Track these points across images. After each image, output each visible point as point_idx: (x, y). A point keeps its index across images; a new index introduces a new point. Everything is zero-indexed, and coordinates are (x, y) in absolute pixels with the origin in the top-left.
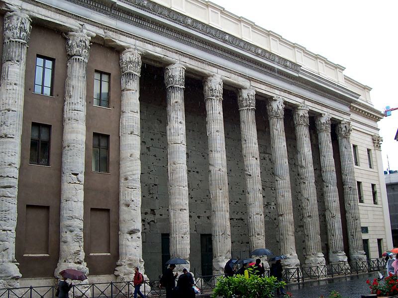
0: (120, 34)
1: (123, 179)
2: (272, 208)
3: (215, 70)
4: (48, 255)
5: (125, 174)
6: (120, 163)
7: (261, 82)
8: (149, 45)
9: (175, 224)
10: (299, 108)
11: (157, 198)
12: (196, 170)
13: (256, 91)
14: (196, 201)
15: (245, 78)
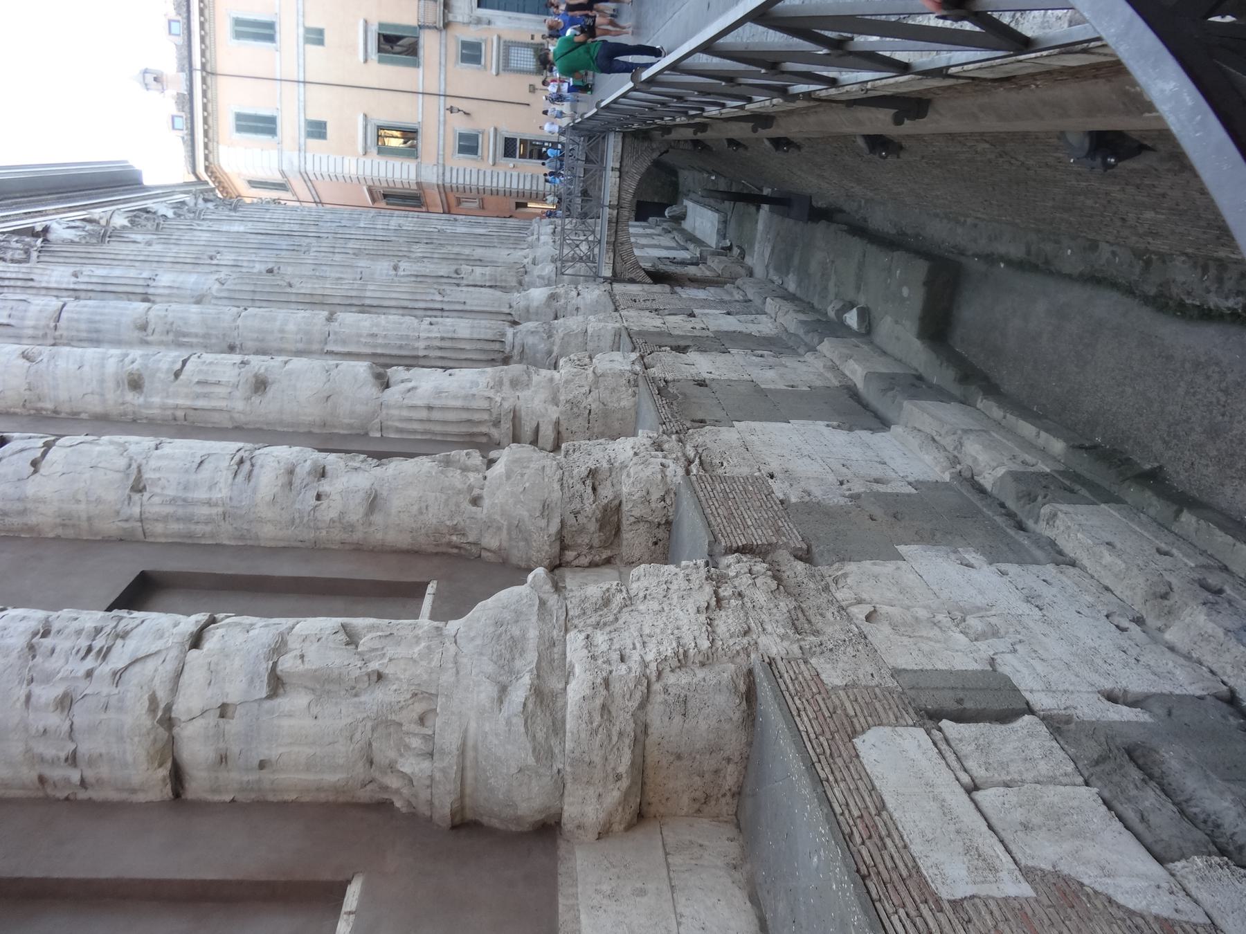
1: (130, 397)
4: (431, 588)
5: (111, 384)
6: (49, 405)
9: (380, 341)
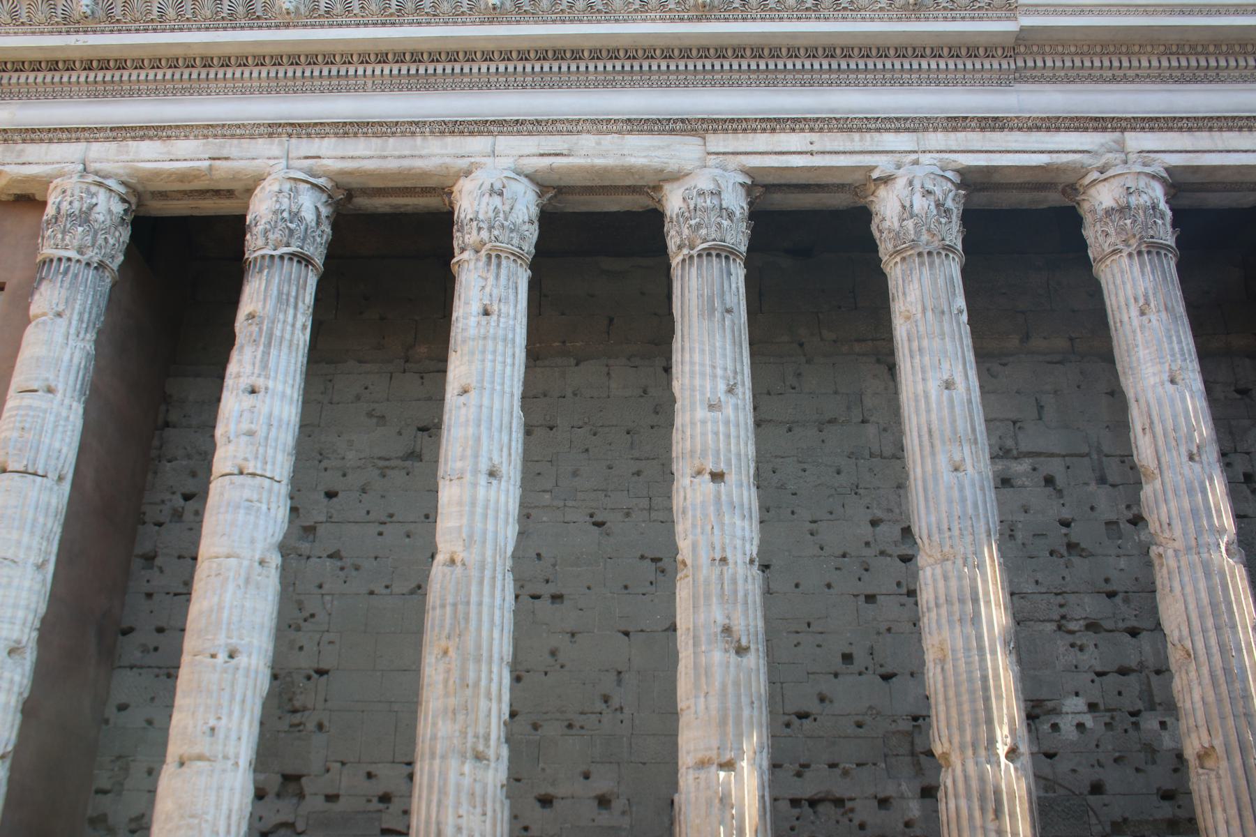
0: (24, 141)
2: (1067, 725)
3: (477, 144)
7: (773, 124)
8: (146, 144)
10: (1087, 181)
11: (320, 727)
12: (547, 590)
13: (747, 172)
14: (535, 727)
15: (660, 132)
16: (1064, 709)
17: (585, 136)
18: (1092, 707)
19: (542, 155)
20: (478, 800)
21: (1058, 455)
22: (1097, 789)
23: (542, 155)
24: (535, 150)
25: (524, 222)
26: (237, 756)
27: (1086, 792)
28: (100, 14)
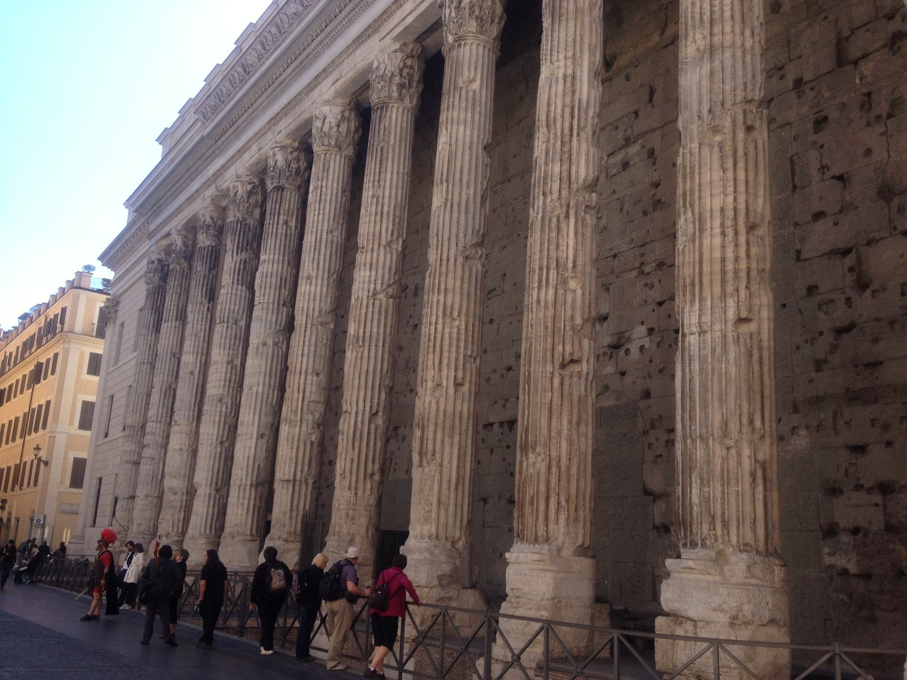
2: (634, 347)
3: (316, 92)
15: (366, 40)
16: (634, 337)
17: (346, 61)
18: (651, 331)
19: (333, 84)
20: (290, 442)
21: (658, 128)
22: (647, 395)
23: (333, 84)
24: (331, 84)
25: (331, 128)
26: (252, 433)
27: (638, 398)
28: (218, 101)
